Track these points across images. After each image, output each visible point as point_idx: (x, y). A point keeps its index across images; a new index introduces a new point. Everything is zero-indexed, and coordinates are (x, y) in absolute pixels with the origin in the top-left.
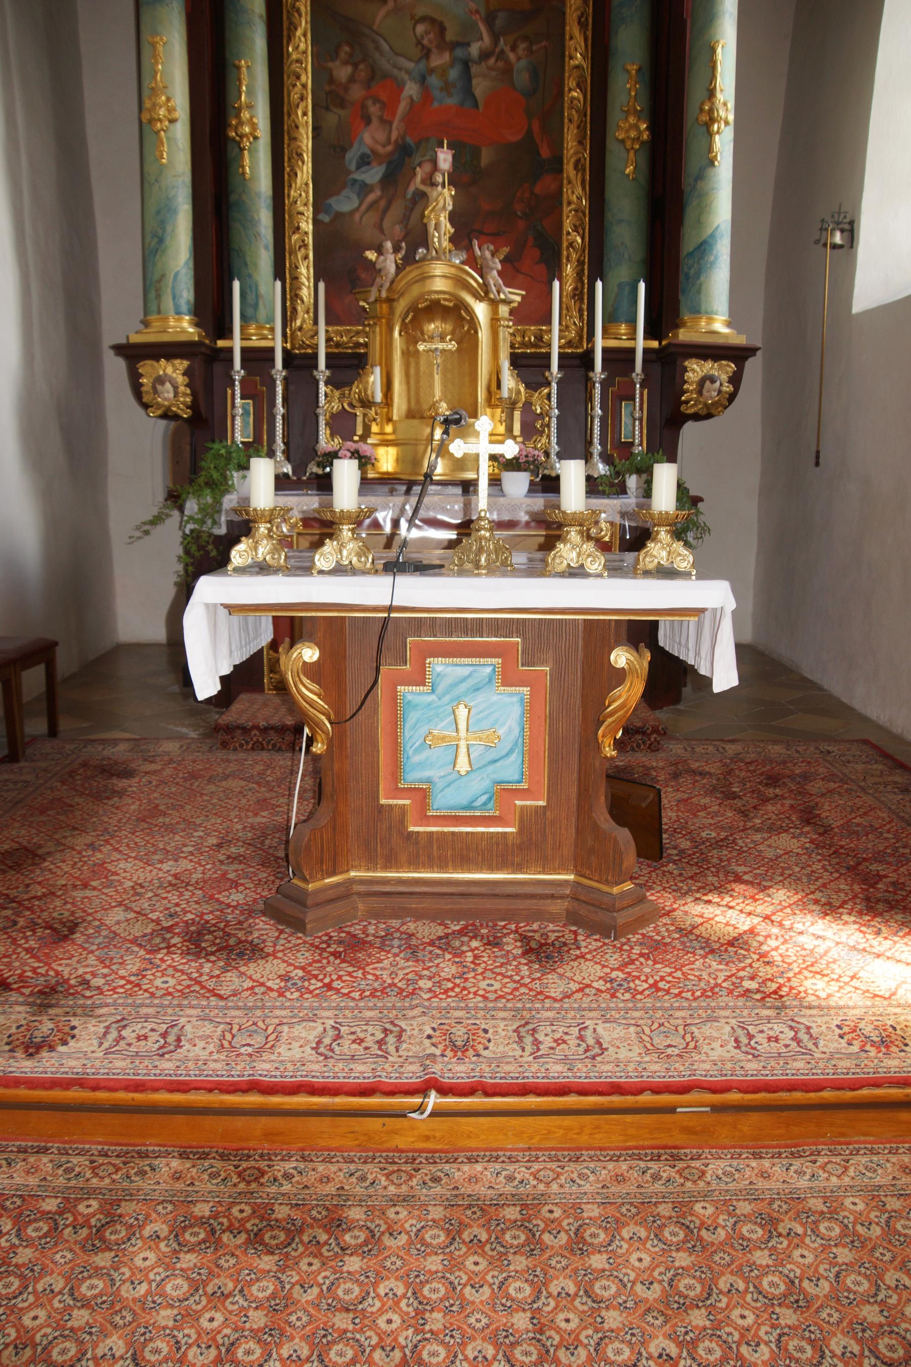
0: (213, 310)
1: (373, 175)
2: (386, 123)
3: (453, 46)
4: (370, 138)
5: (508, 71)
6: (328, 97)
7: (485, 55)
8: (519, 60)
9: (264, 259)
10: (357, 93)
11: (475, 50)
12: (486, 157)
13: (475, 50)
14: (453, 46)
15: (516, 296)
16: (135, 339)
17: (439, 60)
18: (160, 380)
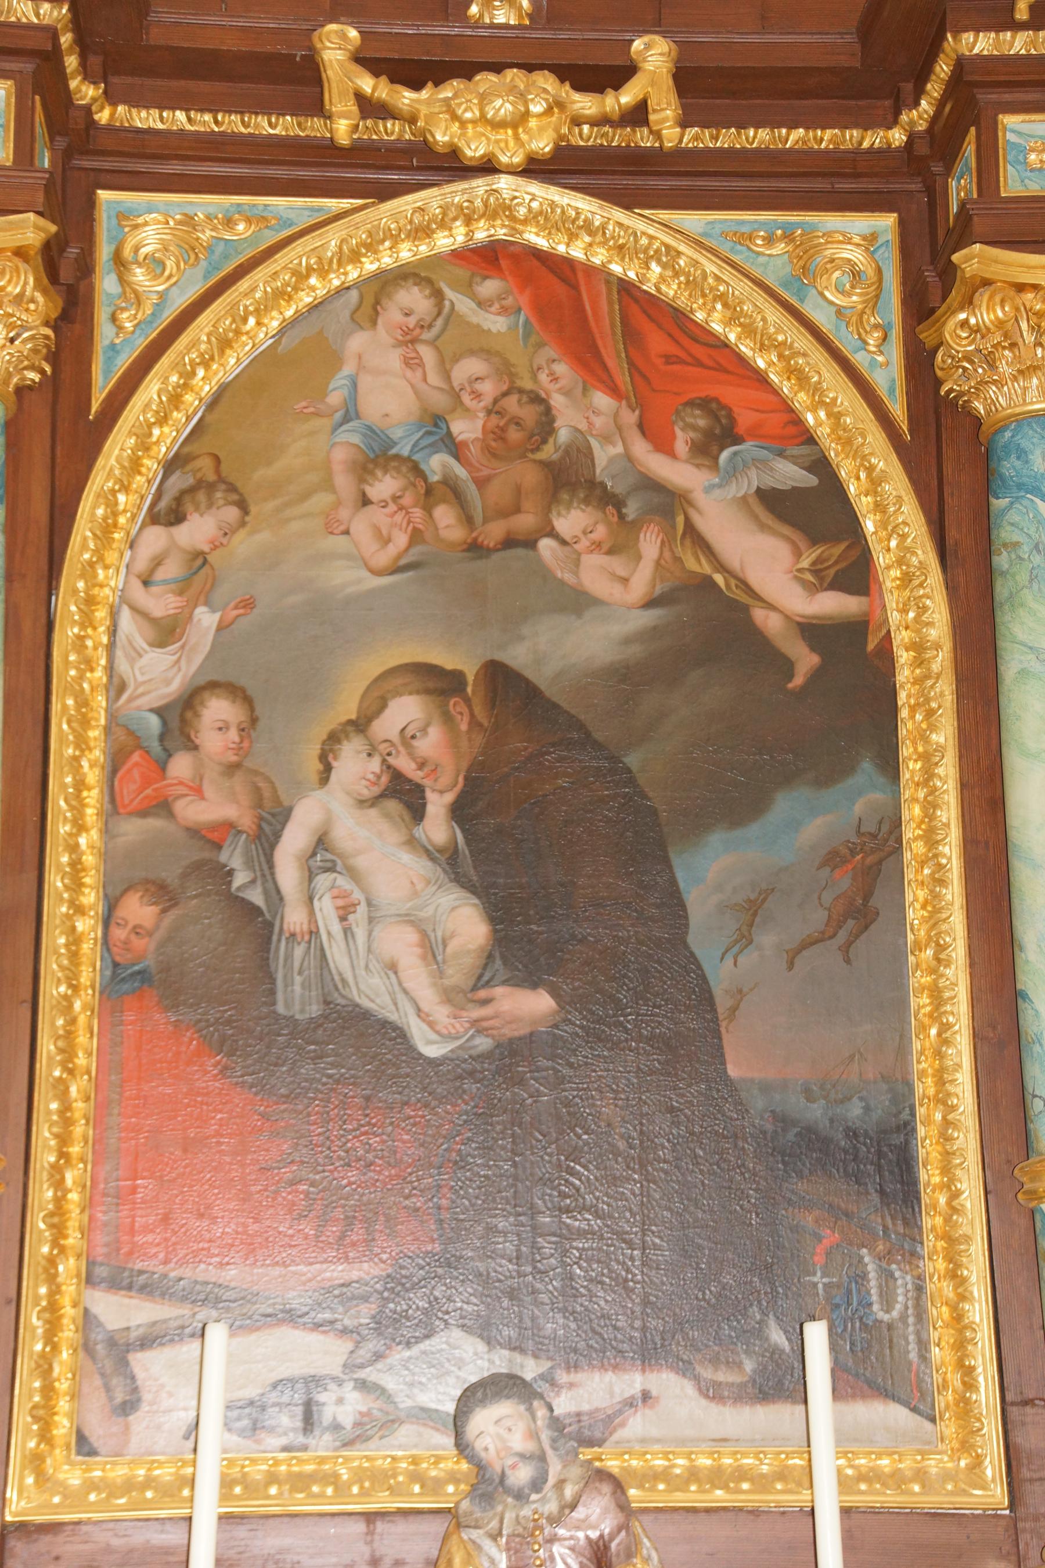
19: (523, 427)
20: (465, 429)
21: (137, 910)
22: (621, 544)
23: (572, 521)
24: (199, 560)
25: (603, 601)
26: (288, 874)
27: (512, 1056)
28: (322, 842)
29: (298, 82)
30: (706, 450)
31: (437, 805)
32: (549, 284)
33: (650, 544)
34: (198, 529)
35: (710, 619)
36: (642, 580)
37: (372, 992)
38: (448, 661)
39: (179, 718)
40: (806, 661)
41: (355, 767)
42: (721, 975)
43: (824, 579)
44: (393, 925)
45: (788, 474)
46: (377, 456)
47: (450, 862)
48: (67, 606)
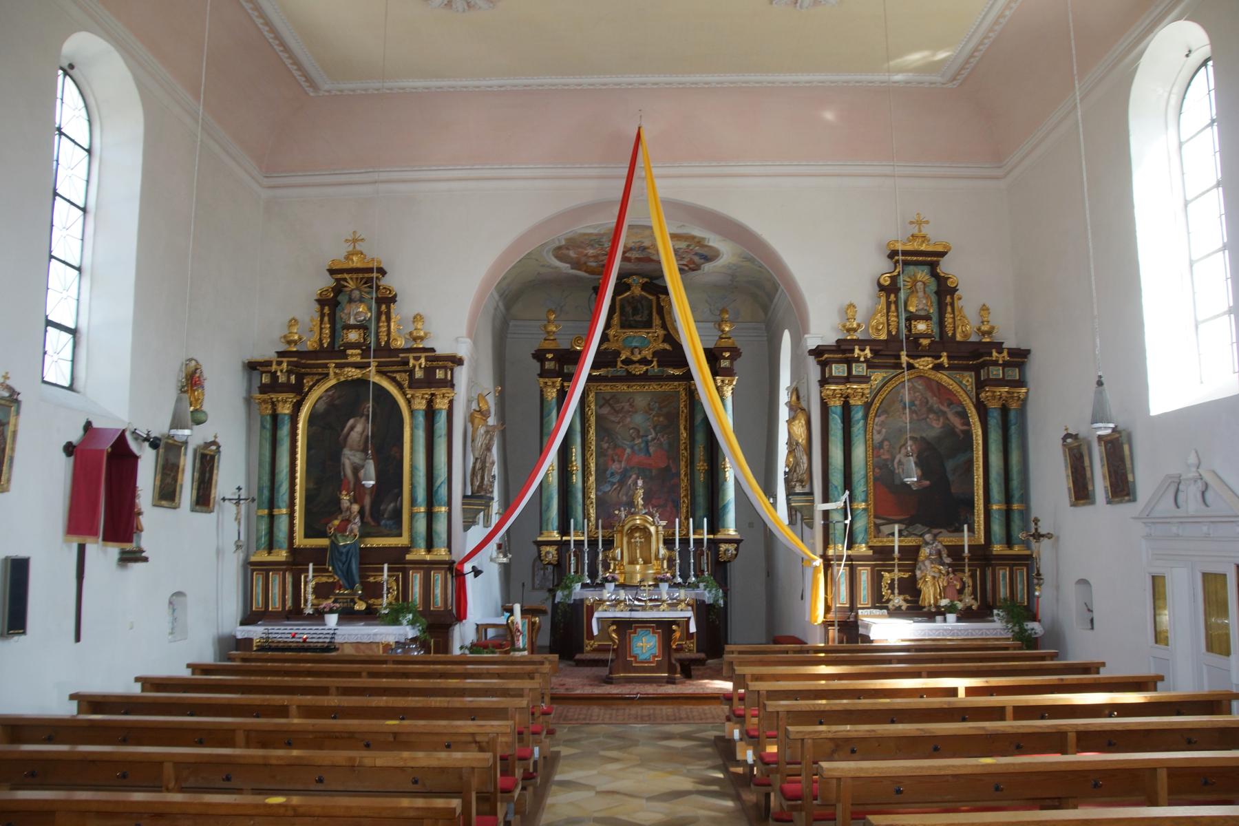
0: (564, 530)
1: (616, 479)
2: (620, 462)
4: (615, 467)
5: (661, 444)
6: (600, 453)
7: (653, 439)
8: (664, 440)
9: (579, 509)
10: (610, 452)
15: (664, 523)
16: (539, 539)
17: (636, 442)
20: (917, 403)
21: (877, 470)
25: (934, 428)
27: (926, 488)
29: (899, 357)
30: (949, 406)
32: (928, 382)
35: (950, 431)
36: (941, 424)
39: (881, 443)
41: (903, 451)
42: (951, 478)
43: (963, 424)
45: (960, 409)
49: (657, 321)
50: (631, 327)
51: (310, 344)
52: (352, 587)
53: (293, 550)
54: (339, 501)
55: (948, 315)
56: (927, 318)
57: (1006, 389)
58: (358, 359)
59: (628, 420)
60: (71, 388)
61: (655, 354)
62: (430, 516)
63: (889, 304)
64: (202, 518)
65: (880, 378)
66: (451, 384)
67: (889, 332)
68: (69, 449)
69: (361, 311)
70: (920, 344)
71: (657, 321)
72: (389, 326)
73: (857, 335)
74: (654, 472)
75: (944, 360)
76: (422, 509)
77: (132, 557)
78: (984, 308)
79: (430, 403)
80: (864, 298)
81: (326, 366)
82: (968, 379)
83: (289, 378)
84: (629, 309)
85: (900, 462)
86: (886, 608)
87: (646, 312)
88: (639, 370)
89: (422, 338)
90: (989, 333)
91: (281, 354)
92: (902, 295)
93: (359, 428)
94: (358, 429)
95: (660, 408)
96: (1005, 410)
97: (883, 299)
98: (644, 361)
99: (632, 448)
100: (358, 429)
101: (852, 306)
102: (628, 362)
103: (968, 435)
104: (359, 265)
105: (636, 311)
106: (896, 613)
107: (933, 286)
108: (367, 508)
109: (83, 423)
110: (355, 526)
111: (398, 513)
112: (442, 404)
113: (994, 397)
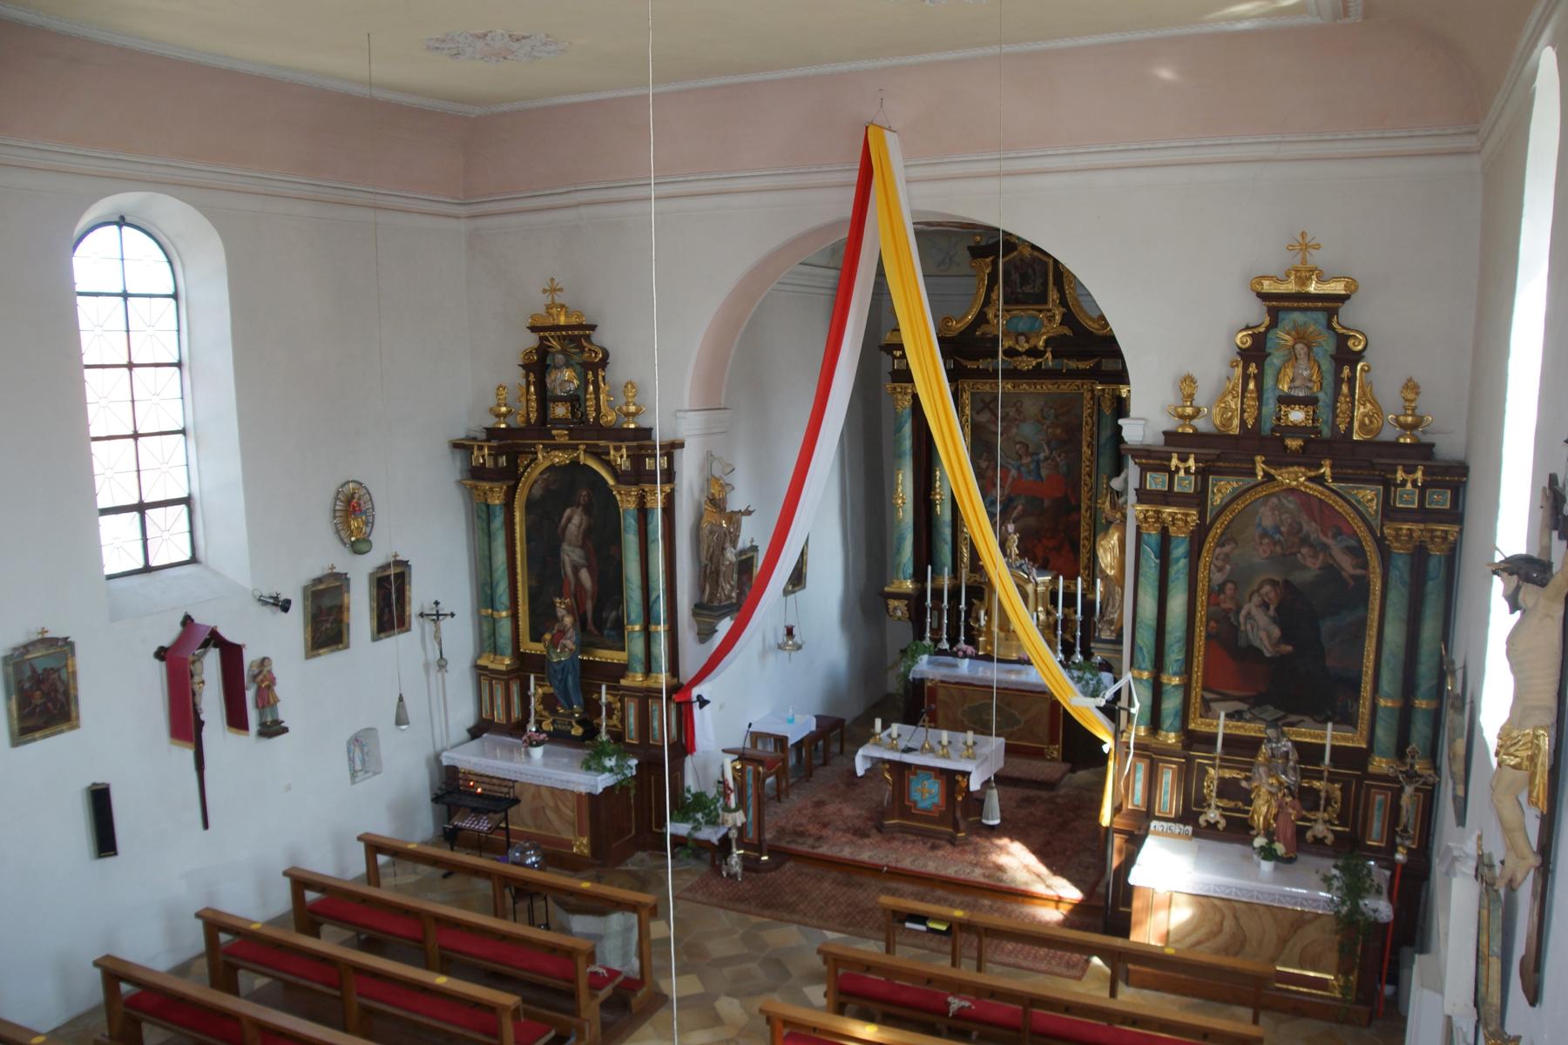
3: (1032, 454)
5: (1057, 466)
7: (1046, 459)
11: (1042, 456)
12: (1047, 503)
13: (1042, 456)
14: (1032, 454)
17: (1025, 460)
18: (895, 609)
19: (1296, 529)
21: (1212, 624)
22: (1315, 556)
23: (1304, 550)
24: (1227, 555)
25: (1312, 566)
26: (1242, 619)
28: (1249, 613)
30: (1334, 537)
31: (1272, 608)
33: (1321, 557)
34: (1227, 549)
35: (1331, 572)
36: (1319, 563)
37: (1257, 643)
38: (1276, 578)
39: (1222, 587)
40: (1352, 583)
41: (1256, 599)
43: (1356, 566)
44: (1261, 630)
45: (1353, 543)
46: (1265, 534)
47: (1274, 620)
48: (1201, 565)
49: (1053, 295)
50: (1018, 302)
51: (519, 421)
52: (571, 707)
53: (518, 655)
54: (553, 605)
55: (1342, 399)
56: (1309, 402)
57: (1422, 526)
58: (565, 440)
59: (1014, 430)
60: (194, 560)
61: (1047, 342)
62: (648, 636)
63: (1246, 378)
64: (396, 643)
65: (1230, 489)
66: (669, 475)
67: (1243, 422)
68: (161, 654)
69: (565, 378)
70: (1286, 447)
71: (1053, 295)
72: (597, 399)
73: (1201, 424)
74: (1047, 503)
75: (1326, 470)
76: (637, 628)
77: (272, 729)
78: (1411, 387)
79: (642, 500)
80: (1213, 367)
81: (534, 446)
82: (1369, 495)
83: (496, 462)
84: (1016, 277)
85: (1249, 616)
86: (1196, 824)
87: (1039, 281)
88: (1027, 364)
89: (634, 414)
90: (1413, 427)
91: (492, 433)
92: (1275, 360)
93: (576, 520)
94: (575, 521)
95: (1057, 417)
96: (1419, 555)
97: (1239, 371)
98: (1034, 352)
99: (1018, 469)
100: (575, 521)
101: (1189, 380)
102: (1010, 353)
103: (1363, 585)
104: (562, 320)
105: (1025, 279)
106: (1206, 832)
107: (1327, 345)
108: (589, 614)
109: (181, 618)
110: (569, 643)
111: (620, 625)
112: (657, 502)
113: (1397, 537)
